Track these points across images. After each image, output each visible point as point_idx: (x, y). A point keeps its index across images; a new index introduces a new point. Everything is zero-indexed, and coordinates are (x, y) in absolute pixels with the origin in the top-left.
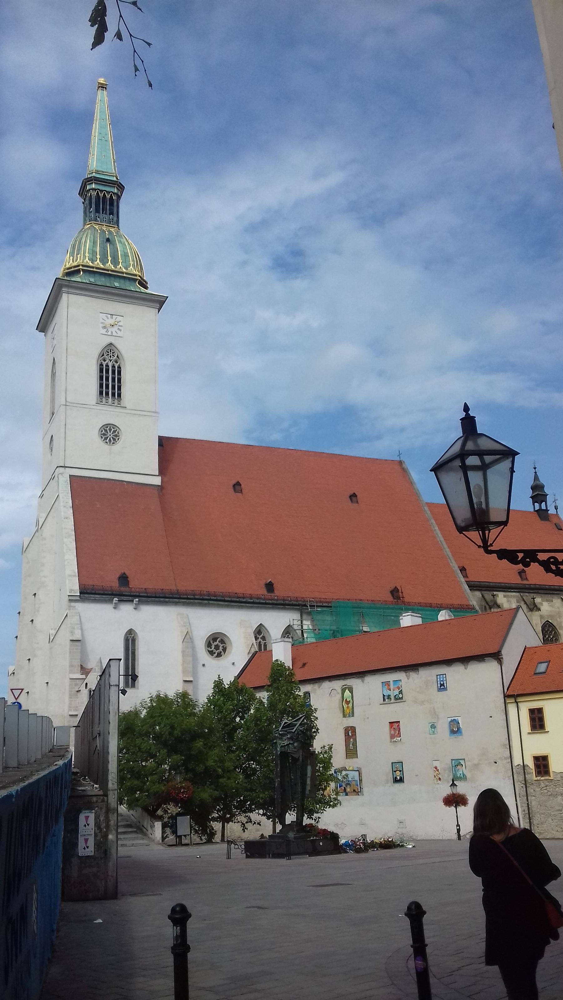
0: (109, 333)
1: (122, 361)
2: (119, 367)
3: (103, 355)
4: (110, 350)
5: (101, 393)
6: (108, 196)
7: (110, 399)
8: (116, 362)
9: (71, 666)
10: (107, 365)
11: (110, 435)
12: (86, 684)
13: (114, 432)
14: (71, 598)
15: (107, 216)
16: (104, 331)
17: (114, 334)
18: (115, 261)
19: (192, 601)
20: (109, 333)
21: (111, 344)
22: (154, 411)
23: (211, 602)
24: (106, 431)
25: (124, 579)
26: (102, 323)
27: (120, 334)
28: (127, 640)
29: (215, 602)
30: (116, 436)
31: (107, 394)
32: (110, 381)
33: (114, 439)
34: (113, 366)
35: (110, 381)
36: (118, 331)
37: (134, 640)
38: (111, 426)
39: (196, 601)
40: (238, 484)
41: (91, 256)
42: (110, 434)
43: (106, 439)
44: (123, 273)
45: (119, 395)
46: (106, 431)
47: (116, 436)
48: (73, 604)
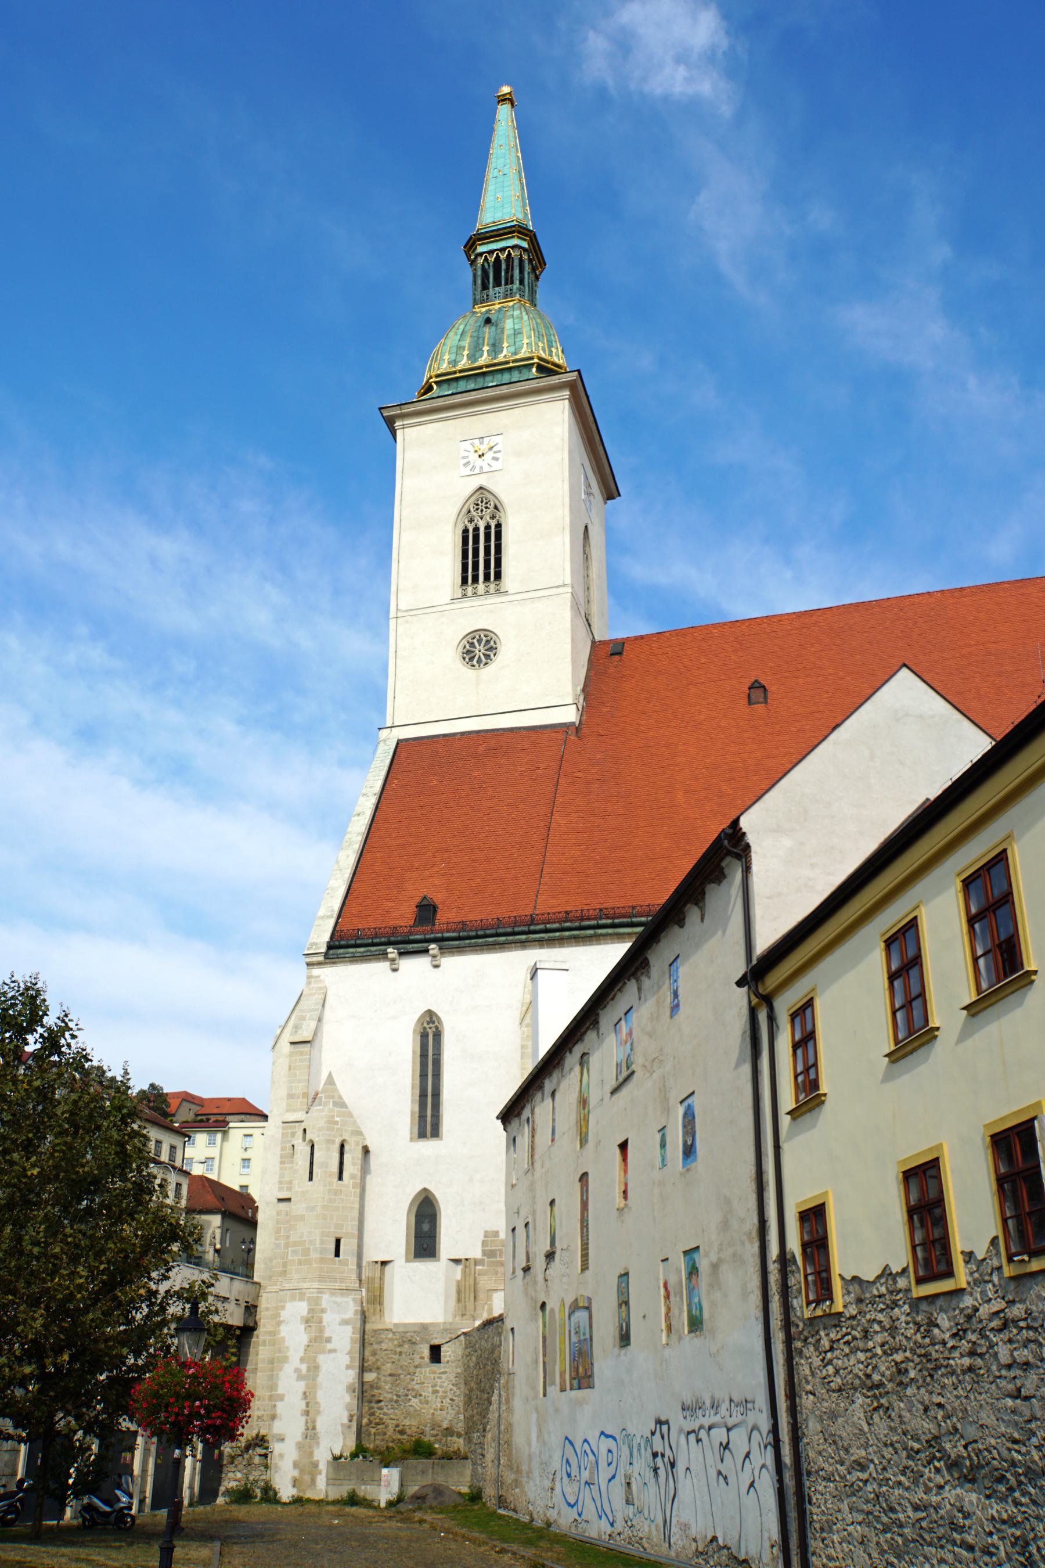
1: (502, 514)
2: (499, 526)
3: (469, 511)
4: (483, 500)
5: (464, 581)
6: (503, 256)
7: (481, 586)
8: (493, 517)
9: (291, 1096)
10: (476, 529)
11: (480, 650)
12: (305, 1130)
13: (488, 642)
14: (309, 960)
15: (501, 289)
16: (467, 471)
17: (486, 469)
18: (496, 348)
19: (557, 934)
20: (477, 471)
21: (481, 488)
22: (561, 583)
23: (600, 931)
24: (472, 644)
25: (427, 911)
26: (463, 458)
27: (496, 465)
28: (424, 1036)
29: (610, 931)
30: (491, 649)
31: (475, 580)
32: (481, 555)
33: (487, 657)
34: (488, 527)
35: (481, 555)
36: (493, 463)
37: (438, 1035)
38: (482, 633)
39: (567, 933)
40: (757, 686)
41: (453, 357)
42: (479, 649)
43: (471, 659)
44: (507, 363)
45: (498, 576)
46: (472, 644)
47: (491, 649)
48: (316, 971)
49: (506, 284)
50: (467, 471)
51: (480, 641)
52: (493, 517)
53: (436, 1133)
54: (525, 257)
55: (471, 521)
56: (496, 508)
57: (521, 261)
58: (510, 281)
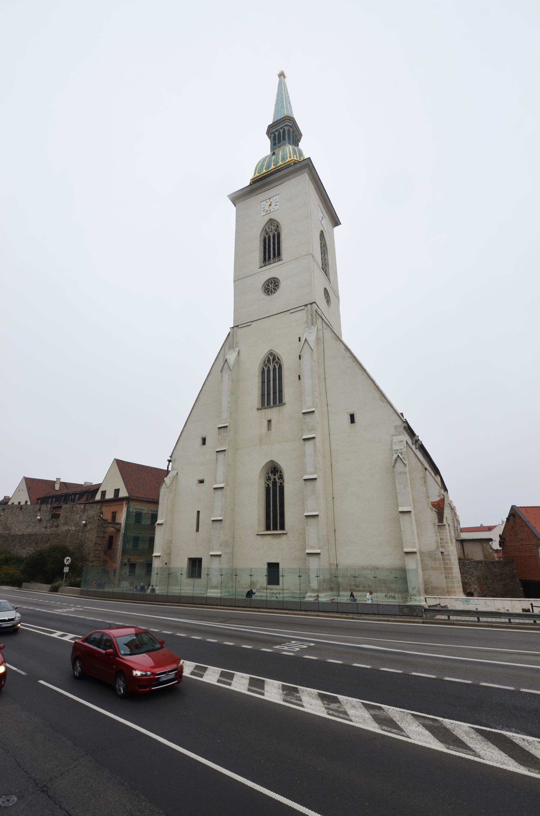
0: (268, 212)
10: (269, 237)
21: (271, 219)
27: (276, 208)
31: (269, 258)
43: (268, 292)
45: (279, 254)
46: (268, 285)
47: (277, 285)
49: (283, 141)
50: (264, 213)
51: (271, 284)
52: (276, 231)
53: (115, 490)
54: (291, 129)
55: (267, 234)
56: (277, 226)
57: (289, 130)
58: (284, 139)
